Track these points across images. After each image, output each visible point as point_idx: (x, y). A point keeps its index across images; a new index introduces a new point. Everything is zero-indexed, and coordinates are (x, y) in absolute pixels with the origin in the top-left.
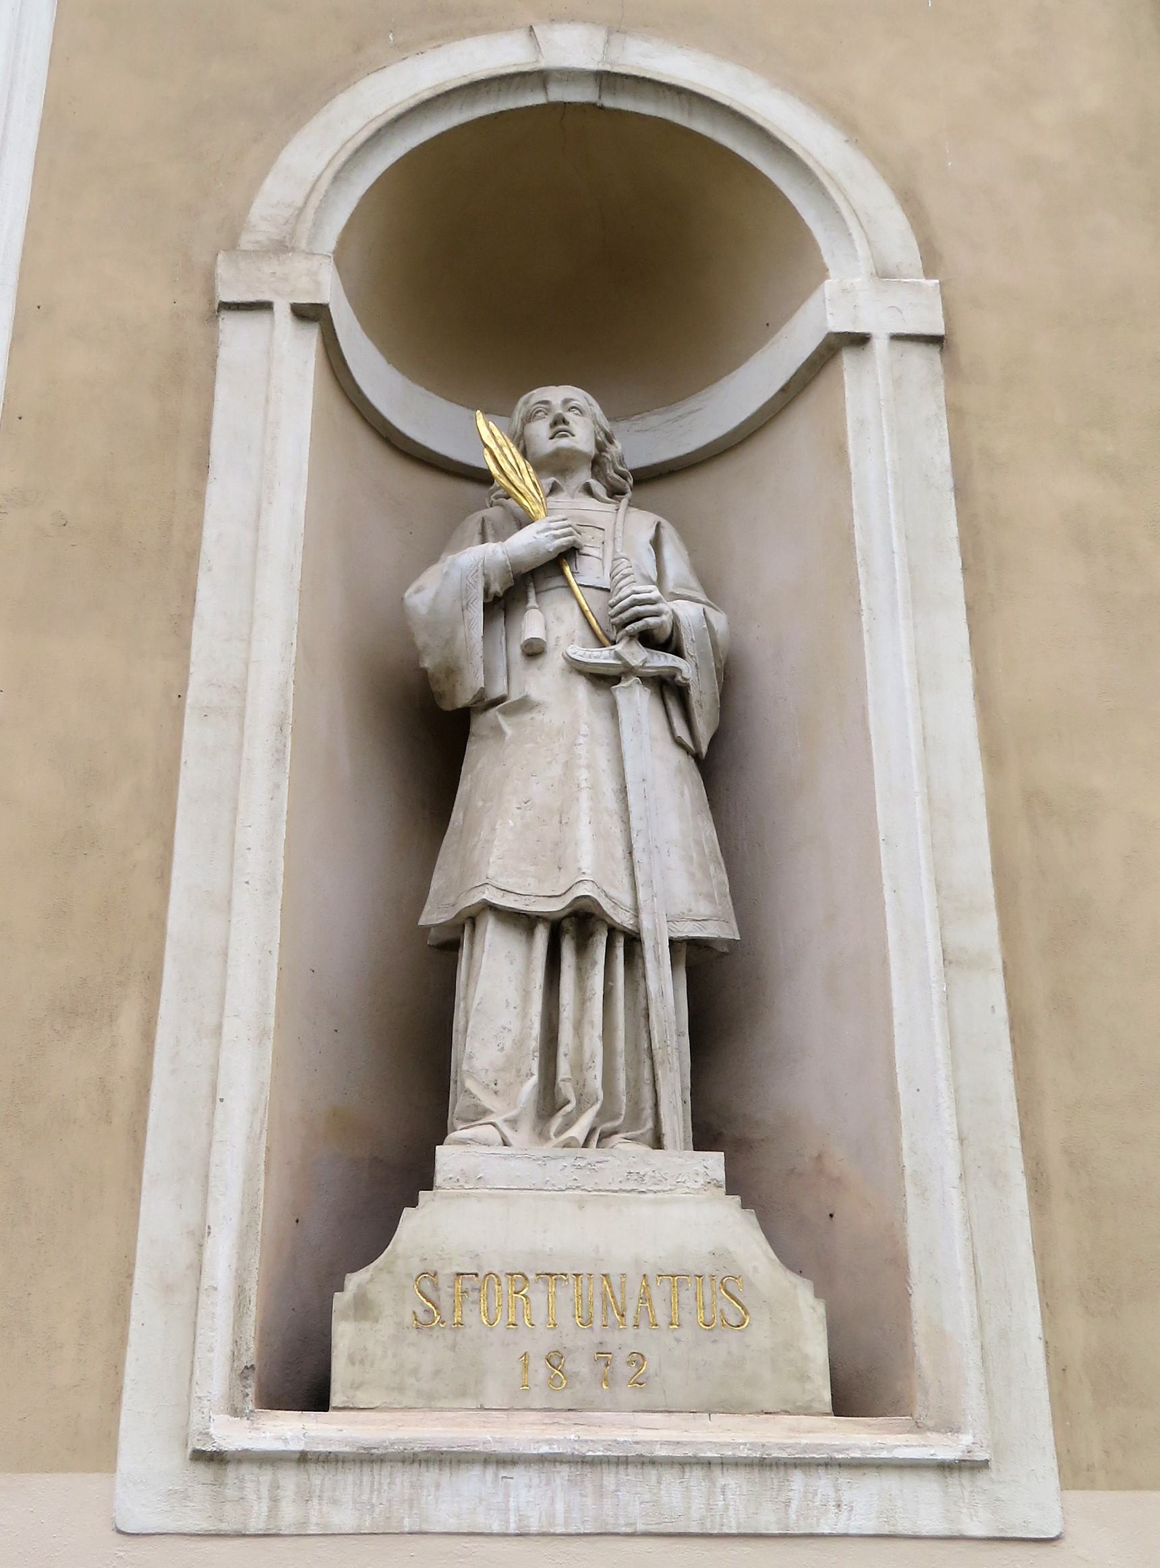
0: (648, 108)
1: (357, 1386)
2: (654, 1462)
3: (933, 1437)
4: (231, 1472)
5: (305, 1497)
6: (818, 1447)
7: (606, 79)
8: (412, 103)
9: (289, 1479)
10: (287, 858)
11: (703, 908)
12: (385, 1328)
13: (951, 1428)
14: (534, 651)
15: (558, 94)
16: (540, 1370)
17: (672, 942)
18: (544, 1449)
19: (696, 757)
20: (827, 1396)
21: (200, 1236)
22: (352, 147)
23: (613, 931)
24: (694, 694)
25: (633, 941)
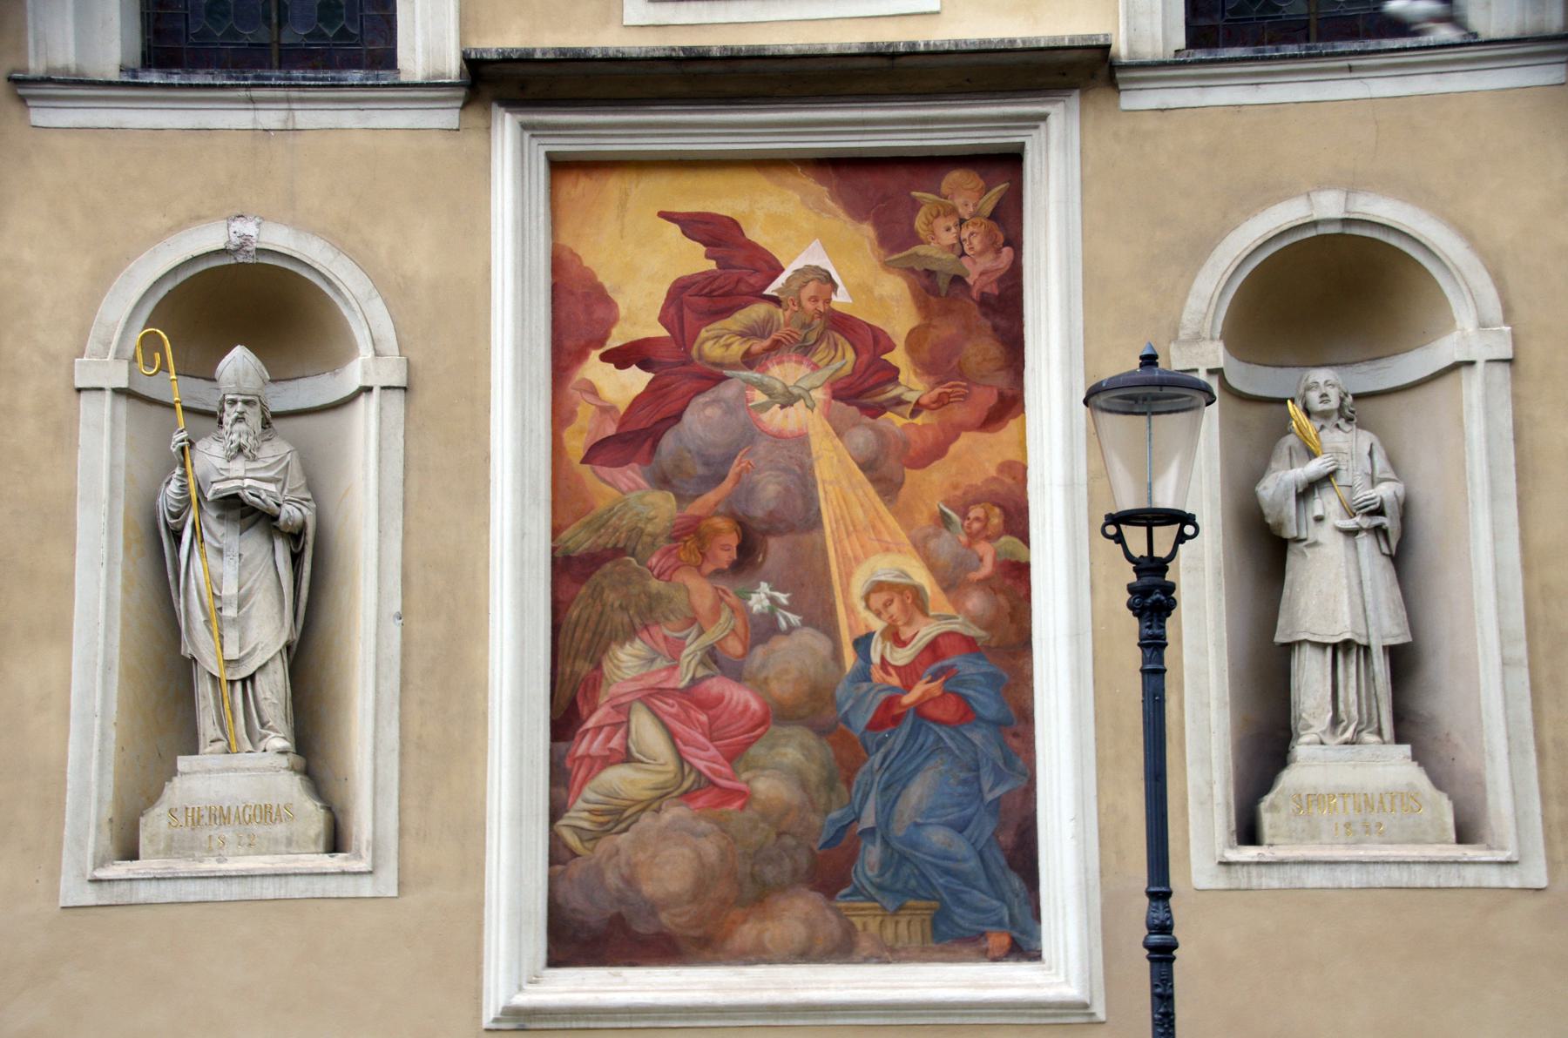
0: (1367, 233)
1: (1274, 836)
2: (1388, 863)
3: (1496, 852)
4: (1233, 868)
5: (1260, 876)
6: (1450, 857)
7: (1346, 222)
8: (1253, 247)
9: (1254, 870)
10: (1228, 632)
11: (1396, 631)
12: (1283, 814)
13: (1503, 849)
14: (1319, 519)
15: (1322, 230)
16: (1342, 830)
17: (1384, 647)
18: (1347, 859)
19: (1390, 556)
20: (1453, 836)
21: (1210, 784)
22: (1226, 276)
23: (1359, 646)
24: (1390, 530)
25: (1367, 649)
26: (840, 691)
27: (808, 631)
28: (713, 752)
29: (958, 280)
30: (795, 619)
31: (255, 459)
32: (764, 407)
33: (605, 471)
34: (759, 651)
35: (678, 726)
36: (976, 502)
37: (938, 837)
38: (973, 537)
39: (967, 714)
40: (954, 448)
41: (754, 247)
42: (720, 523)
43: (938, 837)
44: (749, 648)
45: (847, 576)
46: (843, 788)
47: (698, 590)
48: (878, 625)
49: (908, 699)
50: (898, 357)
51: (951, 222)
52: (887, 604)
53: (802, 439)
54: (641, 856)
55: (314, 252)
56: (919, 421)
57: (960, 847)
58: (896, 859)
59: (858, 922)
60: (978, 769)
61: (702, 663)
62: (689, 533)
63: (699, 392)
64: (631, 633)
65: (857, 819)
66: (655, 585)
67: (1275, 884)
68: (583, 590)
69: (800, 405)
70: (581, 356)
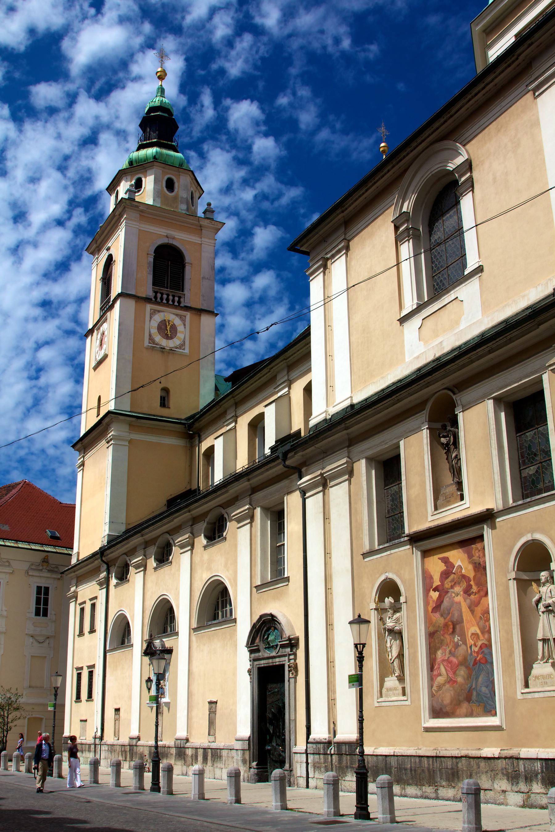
26: (469, 658)
27: (463, 645)
28: (452, 673)
29: (479, 564)
30: (461, 642)
31: (392, 619)
32: (454, 597)
33: (434, 614)
34: (457, 650)
35: (447, 667)
36: (485, 613)
37: (484, 689)
38: (485, 621)
39: (486, 661)
40: (482, 602)
41: (451, 562)
42: (450, 623)
43: (484, 689)
44: (455, 650)
45: (468, 632)
46: (469, 679)
47: (448, 637)
48: (473, 643)
49: (478, 659)
50: (472, 583)
51: (477, 551)
52: (474, 638)
53: (460, 603)
54: (443, 695)
55: (528, 537)
56: (476, 596)
57: (487, 692)
58: (478, 695)
59: (473, 708)
60: (488, 674)
61: (449, 654)
62: (446, 625)
63: (445, 595)
64: (439, 648)
65: (472, 686)
66: (442, 637)
67: (530, 697)
68: (433, 640)
69: (459, 596)
70: (430, 591)
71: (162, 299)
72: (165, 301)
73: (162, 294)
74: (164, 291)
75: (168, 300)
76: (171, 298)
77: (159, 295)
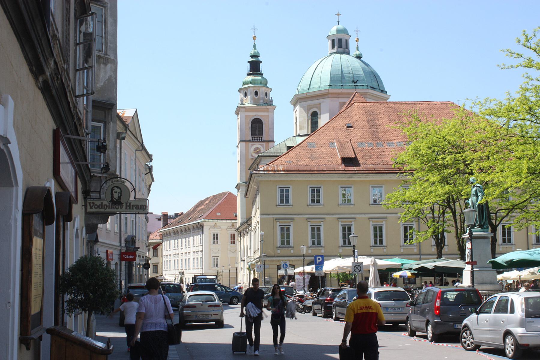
71: (255, 139)
72: (256, 140)
73: (255, 138)
74: (256, 136)
75: (257, 139)
76: (258, 138)
77: (254, 138)
